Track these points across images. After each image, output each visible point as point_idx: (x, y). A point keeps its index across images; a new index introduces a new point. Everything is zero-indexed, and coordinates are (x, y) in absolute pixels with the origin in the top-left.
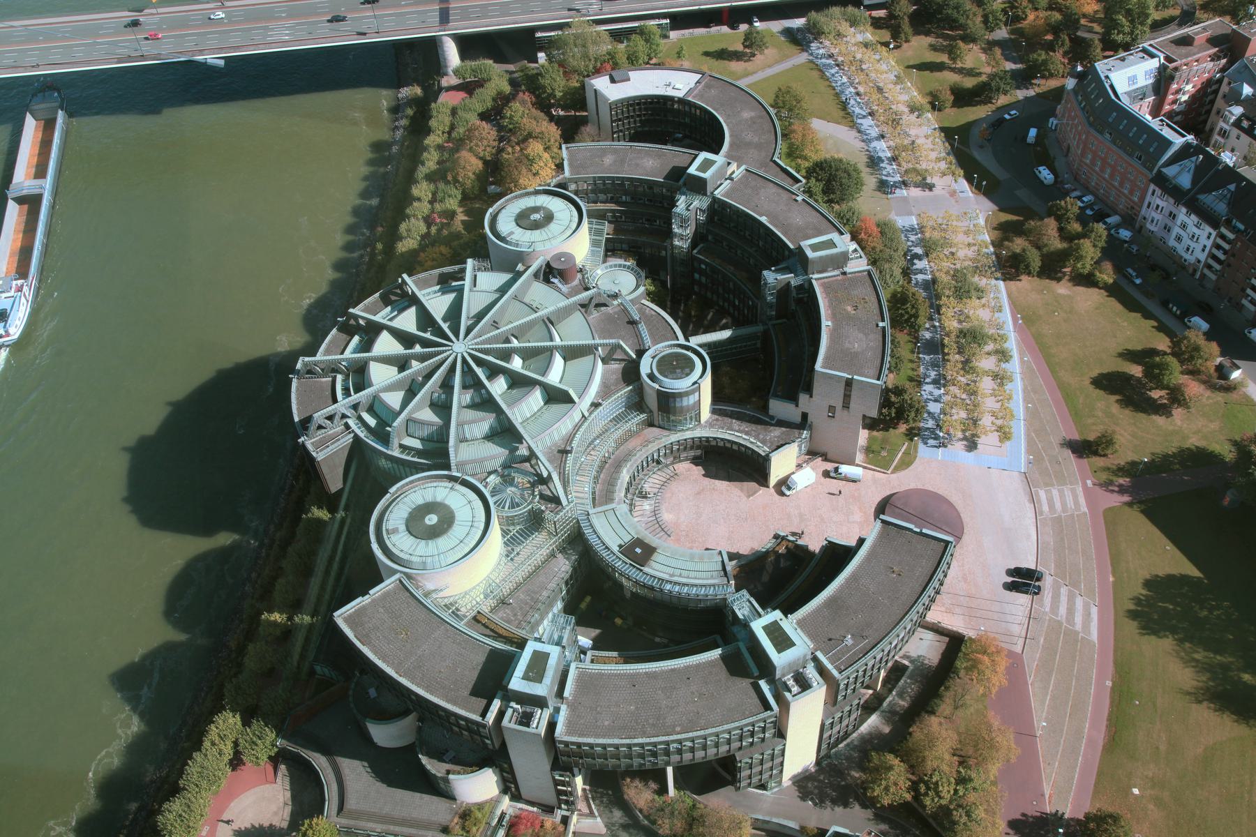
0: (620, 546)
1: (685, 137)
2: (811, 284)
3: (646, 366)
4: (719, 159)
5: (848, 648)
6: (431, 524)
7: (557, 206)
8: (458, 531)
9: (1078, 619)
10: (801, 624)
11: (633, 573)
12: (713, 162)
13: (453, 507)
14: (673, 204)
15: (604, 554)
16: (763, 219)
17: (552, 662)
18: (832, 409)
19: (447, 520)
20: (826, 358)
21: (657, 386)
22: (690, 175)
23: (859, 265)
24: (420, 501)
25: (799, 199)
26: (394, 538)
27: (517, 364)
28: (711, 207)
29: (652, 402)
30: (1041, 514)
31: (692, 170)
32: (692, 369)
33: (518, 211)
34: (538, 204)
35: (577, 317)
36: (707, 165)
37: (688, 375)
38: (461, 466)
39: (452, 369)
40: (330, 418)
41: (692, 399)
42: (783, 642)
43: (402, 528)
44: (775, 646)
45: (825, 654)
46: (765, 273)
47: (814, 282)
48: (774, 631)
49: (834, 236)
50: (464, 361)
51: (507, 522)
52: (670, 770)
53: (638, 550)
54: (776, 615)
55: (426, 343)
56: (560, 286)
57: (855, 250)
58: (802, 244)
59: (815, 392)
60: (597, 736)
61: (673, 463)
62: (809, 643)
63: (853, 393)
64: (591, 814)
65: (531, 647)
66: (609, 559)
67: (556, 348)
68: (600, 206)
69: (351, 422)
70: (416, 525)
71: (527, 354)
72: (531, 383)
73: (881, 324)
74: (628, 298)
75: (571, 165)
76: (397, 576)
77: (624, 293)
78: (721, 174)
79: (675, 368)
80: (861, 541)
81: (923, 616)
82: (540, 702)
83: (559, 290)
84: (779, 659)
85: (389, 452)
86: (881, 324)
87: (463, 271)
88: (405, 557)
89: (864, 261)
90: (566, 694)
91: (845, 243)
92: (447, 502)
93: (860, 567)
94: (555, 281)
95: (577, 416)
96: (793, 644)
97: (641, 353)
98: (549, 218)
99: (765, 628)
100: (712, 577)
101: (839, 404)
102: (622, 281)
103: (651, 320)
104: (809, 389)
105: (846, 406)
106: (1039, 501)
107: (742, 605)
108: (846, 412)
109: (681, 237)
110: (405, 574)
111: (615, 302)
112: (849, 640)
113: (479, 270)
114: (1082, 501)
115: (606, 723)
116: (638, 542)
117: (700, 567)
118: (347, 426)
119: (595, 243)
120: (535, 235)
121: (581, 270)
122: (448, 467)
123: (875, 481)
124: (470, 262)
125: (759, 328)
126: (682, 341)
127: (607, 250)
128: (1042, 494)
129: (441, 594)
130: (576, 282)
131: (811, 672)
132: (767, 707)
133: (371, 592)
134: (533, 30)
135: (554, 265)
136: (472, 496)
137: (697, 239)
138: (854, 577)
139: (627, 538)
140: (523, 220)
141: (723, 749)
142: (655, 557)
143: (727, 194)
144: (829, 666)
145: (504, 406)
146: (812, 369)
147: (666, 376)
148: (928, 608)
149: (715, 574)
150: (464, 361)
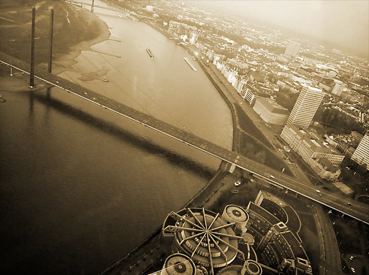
7: (242, 213)
16: (290, 246)
27: (217, 243)
28: (279, 235)
36: (281, 225)
40: (171, 228)
46: (285, 260)
49: (306, 261)
67: (227, 245)
89: (311, 272)
95: (224, 265)
97: (246, 259)
102: (250, 240)
120: (235, 217)
126: (256, 262)
140: (234, 212)
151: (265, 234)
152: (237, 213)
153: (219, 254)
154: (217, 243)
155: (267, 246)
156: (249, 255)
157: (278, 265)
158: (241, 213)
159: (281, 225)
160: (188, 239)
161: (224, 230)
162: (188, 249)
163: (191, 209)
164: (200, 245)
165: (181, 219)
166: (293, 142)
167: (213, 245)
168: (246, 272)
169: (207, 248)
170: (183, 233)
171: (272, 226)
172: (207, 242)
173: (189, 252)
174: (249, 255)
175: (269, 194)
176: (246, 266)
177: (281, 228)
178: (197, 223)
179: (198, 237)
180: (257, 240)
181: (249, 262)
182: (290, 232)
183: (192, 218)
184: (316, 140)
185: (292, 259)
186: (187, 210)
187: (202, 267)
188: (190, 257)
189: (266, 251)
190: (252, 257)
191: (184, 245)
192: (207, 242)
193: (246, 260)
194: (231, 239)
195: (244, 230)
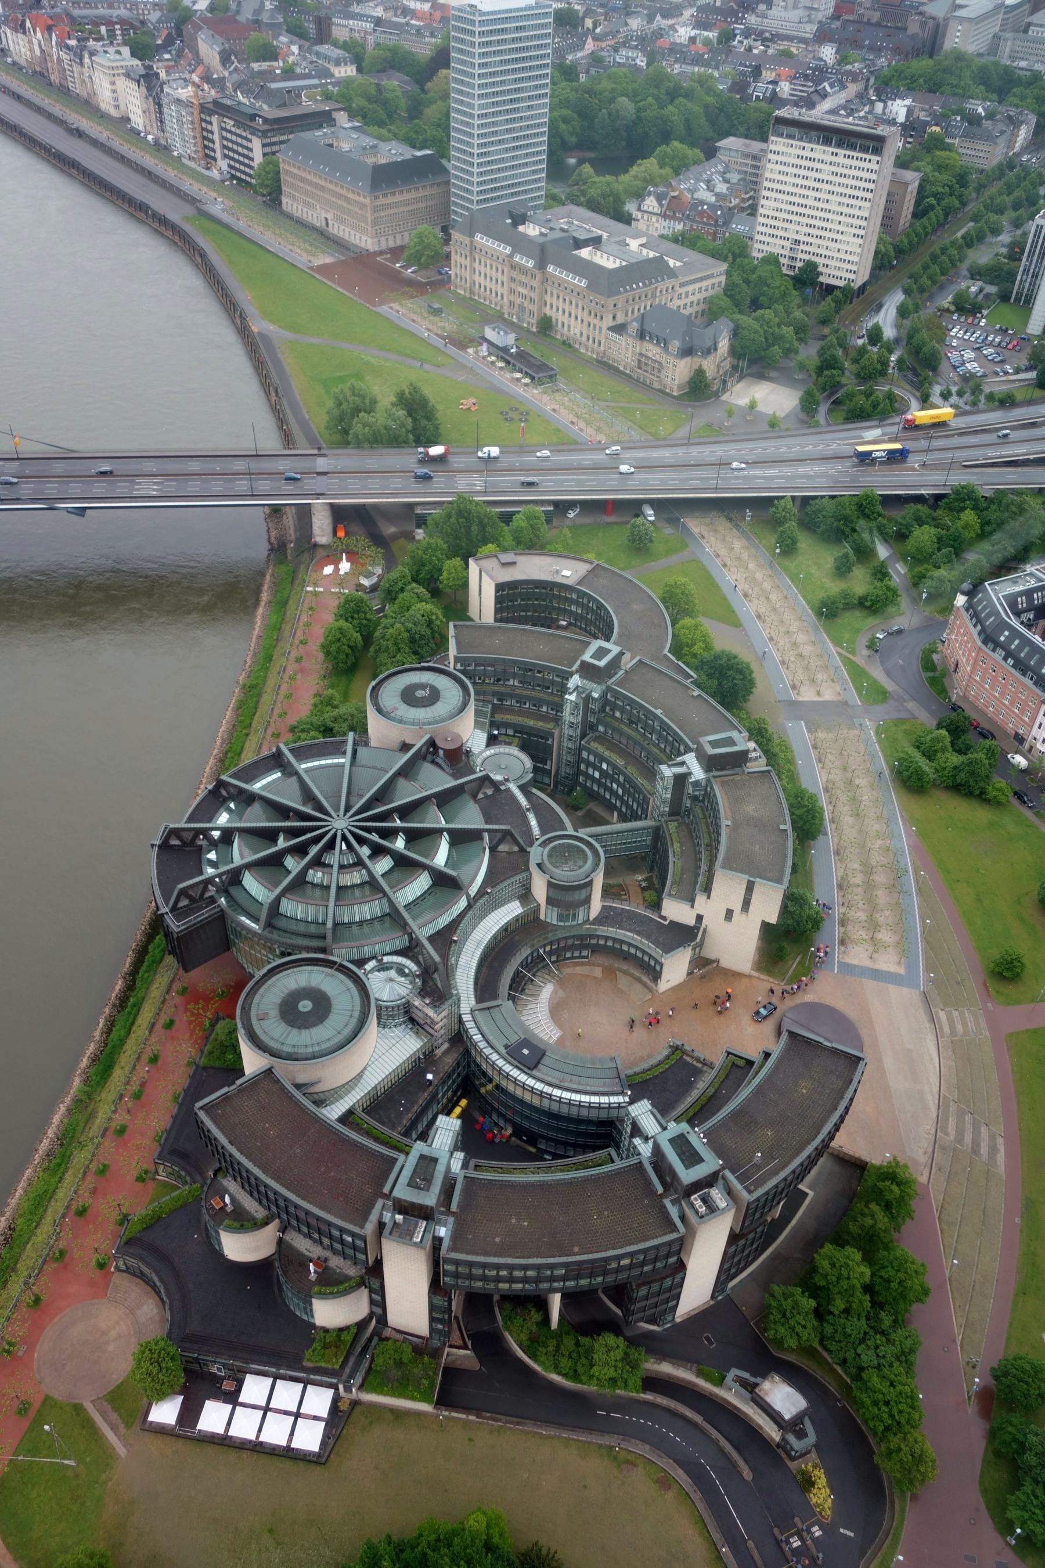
0: (506, 1047)
1: (570, 624)
3: (536, 853)
5: (758, 1167)
6: (306, 1011)
9: (984, 1150)
11: (523, 1078)
14: (564, 690)
15: (488, 1051)
16: (658, 712)
17: (441, 1169)
18: (729, 914)
22: (583, 663)
23: (758, 764)
28: (604, 695)
31: (587, 657)
32: (585, 861)
33: (402, 687)
37: (580, 867)
39: (331, 846)
41: (583, 894)
42: (691, 1158)
43: (274, 1013)
44: (683, 1161)
45: (733, 1172)
46: (663, 768)
47: (713, 780)
48: (680, 1143)
49: (734, 734)
52: (556, 1302)
53: (526, 1052)
54: (684, 1127)
58: (701, 740)
60: (486, 1254)
63: (754, 896)
64: (466, 1347)
65: (419, 1148)
66: (494, 1057)
67: (439, 832)
71: (413, 836)
78: (615, 663)
81: (831, 1136)
82: (426, 1214)
86: (782, 827)
87: (345, 742)
89: (763, 760)
90: (454, 1207)
95: (463, 903)
98: (434, 696)
99: (672, 1141)
101: (737, 907)
102: (508, 765)
103: (537, 807)
106: (940, 1022)
107: (642, 1112)
108: (744, 916)
114: (983, 1024)
115: (497, 1240)
116: (526, 1043)
119: (478, 725)
124: (351, 735)
126: (571, 831)
128: (942, 1015)
129: (312, 1090)
131: (717, 1194)
132: (674, 1228)
134: (411, 506)
137: (588, 728)
139: (514, 1039)
140: (409, 696)
141: (622, 1276)
143: (619, 683)
145: (387, 888)
148: (837, 1128)
150: (344, 838)
151: (557, 720)
152: (420, 693)
153: (422, 883)
154: (400, 844)
155: (585, 754)
156: (533, 822)
157: (646, 801)
158: (436, 684)
159: (601, 653)
160: (282, 894)
161: (402, 782)
162: (302, 928)
163: (234, 776)
164: (340, 888)
165: (216, 834)
166: (512, 291)
167: (384, 864)
168: (550, 885)
169: (372, 884)
170: (250, 883)
171: (571, 674)
172: (359, 863)
173: (312, 936)
174: (533, 822)
175: (506, 557)
176: (539, 865)
177: (602, 663)
178: (283, 811)
179: (318, 862)
180: (535, 745)
181: (544, 844)
182: (640, 661)
184: (596, 242)
185: (686, 752)
187: (386, 959)
188: (323, 950)
190: (548, 822)
192: (359, 863)
193: (531, 845)
194: (444, 799)
195: (473, 738)
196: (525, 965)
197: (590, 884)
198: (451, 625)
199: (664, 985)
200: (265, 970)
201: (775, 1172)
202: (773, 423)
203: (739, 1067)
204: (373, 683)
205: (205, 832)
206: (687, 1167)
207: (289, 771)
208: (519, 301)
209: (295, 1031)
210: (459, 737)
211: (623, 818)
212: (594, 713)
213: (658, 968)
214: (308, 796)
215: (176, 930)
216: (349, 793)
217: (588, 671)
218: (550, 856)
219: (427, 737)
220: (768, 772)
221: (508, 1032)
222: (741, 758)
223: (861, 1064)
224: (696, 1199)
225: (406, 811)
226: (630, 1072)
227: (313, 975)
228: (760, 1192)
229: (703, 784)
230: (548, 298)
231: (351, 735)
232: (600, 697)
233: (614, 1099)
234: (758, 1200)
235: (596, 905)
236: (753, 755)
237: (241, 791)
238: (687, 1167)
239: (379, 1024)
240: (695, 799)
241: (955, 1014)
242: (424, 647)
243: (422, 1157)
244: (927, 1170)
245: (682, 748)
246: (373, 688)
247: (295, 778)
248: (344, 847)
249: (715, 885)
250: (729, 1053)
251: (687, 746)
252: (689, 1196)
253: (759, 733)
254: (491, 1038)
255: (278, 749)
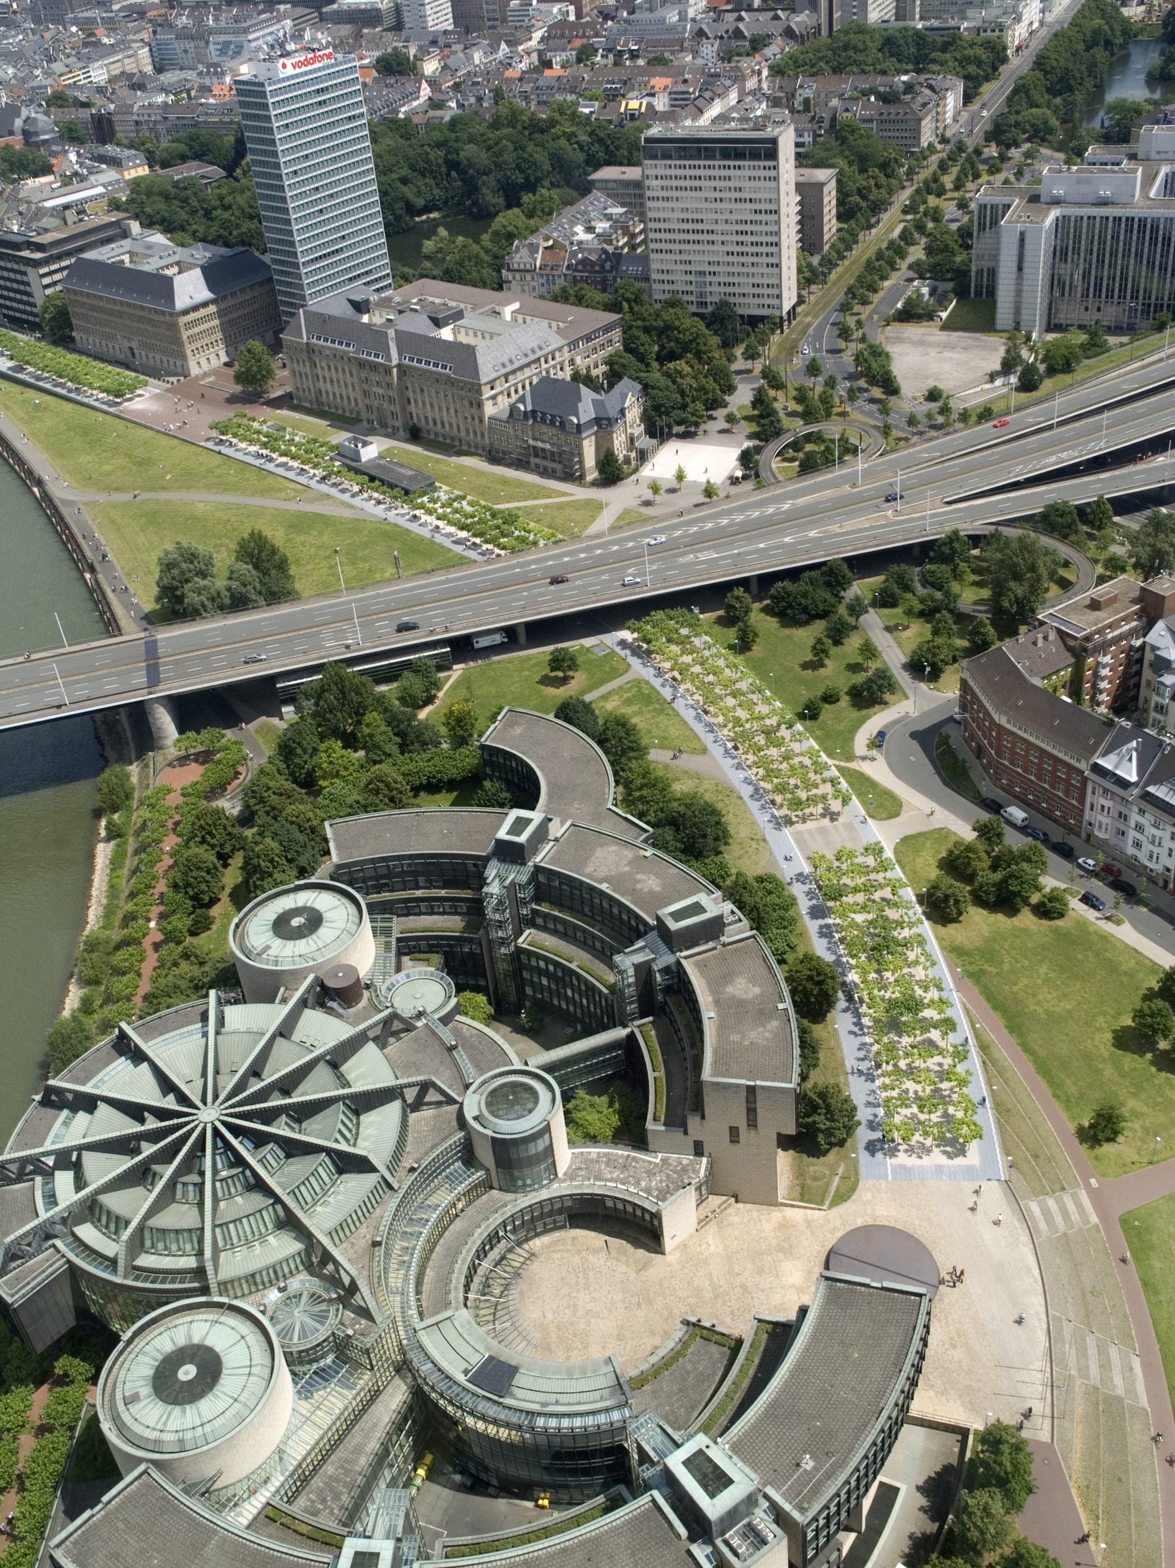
0: (466, 1372)
2: (679, 963)
3: (473, 1104)
4: (536, 816)
6: (190, 1377)
7: (324, 902)
8: (228, 1383)
10: (737, 1449)
12: (529, 821)
13: (217, 1349)
14: (483, 882)
16: (604, 887)
18: (734, 1133)
19: (210, 1367)
20: (715, 1062)
21: (489, 1133)
22: (499, 842)
23: (739, 930)
24: (169, 1348)
25: (647, 854)
26: (134, 1409)
29: (485, 1155)
30: (1039, 1232)
31: (502, 834)
33: (274, 917)
34: (300, 904)
35: (370, 1048)
37: (530, 1112)
38: (224, 1287)
39: (200, 1144)
41: (541, 1144)
42: (715, 1480)
43: (146, 1390)
44: (705, 1487)
47: (684, 962)
48: (700, 1465)
49: (702, 898)
50: (216, 1133)
51: (295, 1360)
54: (700, 1441)
55: (161, 1114)
56: (341, 1011)
57: (733, 912)
58: (660, 913)
59: (708, 1111)
61: (527, 1240)
62: (754, 1476)
63: (759, 1105)
68: (386, 896)
69: (58, 1243)
70: (167, 1386)
72: (311, 1149)
73: (781, 1006)
74: (436, 1016)
75: (337, 847)
76: (142, 1467)
77: (429, 1010)
78: (541, 834)
79: (512, 1104)
80: (803, 1311)
81: (904, 1408)
83: (339, 1016)
84: (713, 1507)
85: (118, 1280)
86: (781, 1006)
88: (154, 1435)
89: (745, 922)
91: (714, 905)
92: (208, 1343)
93: (807, 1350)
94: (334, 1005)
96: (730, 1482)
98: (315, 920)
99: (687, 1463)
100: (602, 1399)
101: (742, 1123)
102: (423, 990)
104: (698, 1107)
105: (752, 1123)
106: (1032, 1217)
108: (753, 1132)
109: (500, 925)
110: (155, 1463)
111: (419, 1024)
112: (808, 1463)
113: (229, 1002)
117: (583, 1385)
118: (58, 1251)
121: (368, 987)
122: (205, 1290)
123: (809, 1223)
125: (619, 1033)
127: (400, 954)
128: (1034, 1207)
130: (364, 1003)
133: (105, 1499)
135: (331, 983)
136: (245, 1328)
138: (799, 1368)
139: (476, 1360)
140: (282, 927)
142: (519, 1380)
143: (553, 861)
144: (787, 1507)
146: (698, 1085)
147: (497, 1117)
148: (909, 1396)
149: (605, 1392)
150: (216, 1133)
152: (296, 922)
158: (317, 906)
165: (50, 1161)
171: (486, 860)
176: (476, 1118)
178: (135, 1111)
183: (102, 1107)
185: (646, 933)
186: (49, 1091)
188: (205, 1290)
189: (532, 984)
191: (146, 1260)
196: (482, 1253)
197: (547, 1129)
198: (327, 824)
199: (669, 1243)
200: (129, 1334)
201: (830, 1475)
202: (709, 491)
203: (780, 1336)
204: (236, 920)
205: (35, 1160)
206: (712, 1495)
207: (138, 1056)
208: (376, 403)
209: (178, 1409)
210: (353, 970)
211: (589, 1032)
212: (524, 903)
213: (656, 1223)
214: (166, 1085)
215: (9, 1300)
216: (217, 1072)
217: (510, 853)
218: (489, 1104)
219: (311, 977)
220: (753, 937)
221: (465, 1351)
222: (714, 928)
223: (925, 1301)
224: (734, 1536)
225: (286, 1085)
226: (634, 1373)
227: (194, 1325)
228: (817, 1507)
229: (674, 968)
230: (411, 395)
231: (212, 993)
232: (529, 883)
233: (616, 1416)
234: (815, 1519)
235: (564, 1156)
236: (731, 918)
237: (77, 1094)
238: (712, 1495)
239: (293, 1373)
240: (668, 990)
241: (1051, 1203)
242: (300, 859)
243: (358, 1555)
244: (1048, 1421)
245: (641, 928)
246: (237, 926)
247: (145, 1064)
248: (220, 1144)
249: (706, 1100)
250: (760, 1321)
251: (645, 923)
252: (723, 1533)
253: (737, 893)
254: (444, 1365)
255: (121, 1030)
